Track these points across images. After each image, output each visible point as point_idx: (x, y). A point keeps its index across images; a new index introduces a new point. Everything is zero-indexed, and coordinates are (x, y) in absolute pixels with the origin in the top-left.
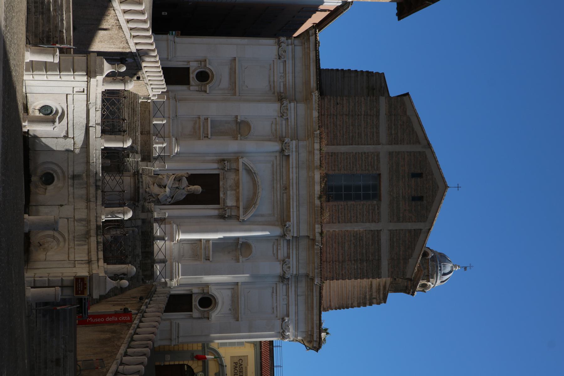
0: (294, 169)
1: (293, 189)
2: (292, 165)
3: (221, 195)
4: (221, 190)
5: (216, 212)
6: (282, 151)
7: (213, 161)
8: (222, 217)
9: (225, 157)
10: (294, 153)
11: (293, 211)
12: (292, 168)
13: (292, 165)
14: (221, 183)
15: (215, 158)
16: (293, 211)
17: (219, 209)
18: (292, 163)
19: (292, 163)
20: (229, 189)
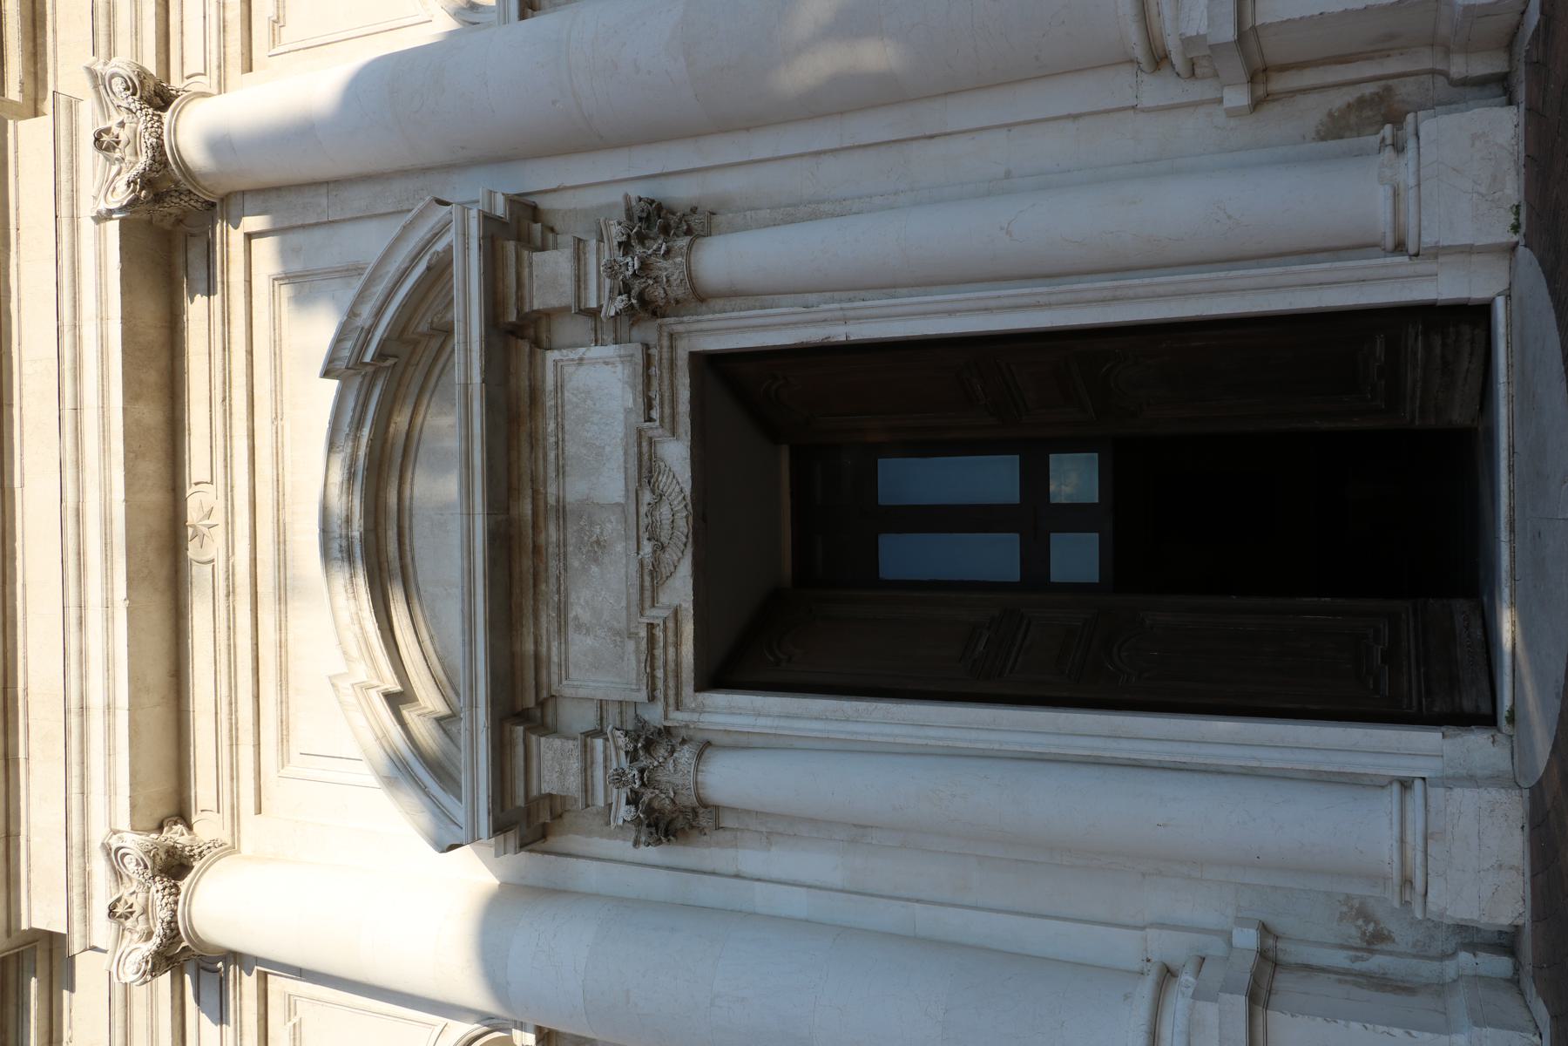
0: (96, 701)
1: (107, 521)
2: (110, 730)
3: (676, 454)
4: (676, 512)
5: (719, 259)
6: (174, 867)
7: (774, 825)
8: (656, 223)
9: (652, 853)
10: (98, 834)
11: (102, 319)
12: (109, 708)
13: (110, 730)
14: (680, 590)
15: (750, 859)
16: (102, 319)
17: (699, 297)
18: (110, 752)
19: (110, 752)
20: (611, 527)
